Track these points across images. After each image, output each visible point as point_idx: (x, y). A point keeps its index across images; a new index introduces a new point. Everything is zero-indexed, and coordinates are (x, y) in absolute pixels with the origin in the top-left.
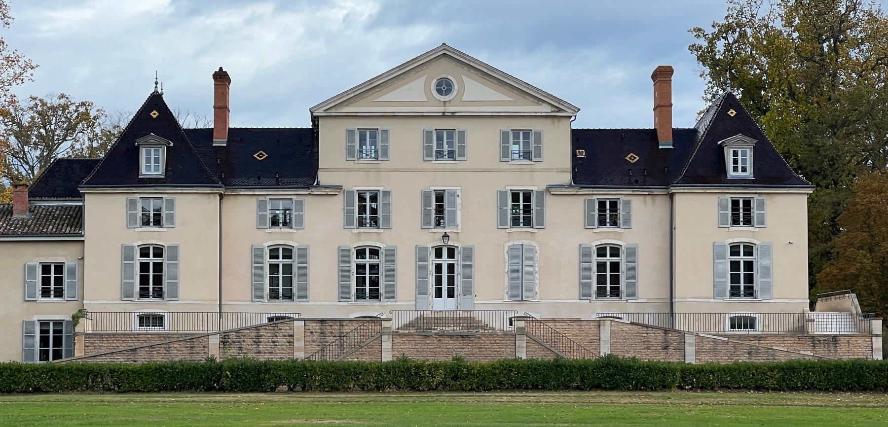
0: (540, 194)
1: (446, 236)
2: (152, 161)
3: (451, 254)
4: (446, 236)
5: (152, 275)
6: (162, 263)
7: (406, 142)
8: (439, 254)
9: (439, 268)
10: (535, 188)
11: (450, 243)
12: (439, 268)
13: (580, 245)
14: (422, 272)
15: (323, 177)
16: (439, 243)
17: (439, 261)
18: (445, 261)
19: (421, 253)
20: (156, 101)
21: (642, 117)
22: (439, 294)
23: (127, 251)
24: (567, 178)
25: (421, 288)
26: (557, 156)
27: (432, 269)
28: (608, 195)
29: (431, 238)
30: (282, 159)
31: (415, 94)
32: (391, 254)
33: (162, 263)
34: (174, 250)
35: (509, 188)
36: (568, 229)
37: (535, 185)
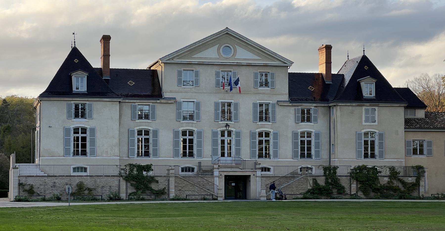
0: (273, 105)
1: (227, 125)
2: (80, 82)
3: (229, 134)
4: (227, 125)
5: (81, 144)
6: (86, 137)
7: (208, 77)
8: (223, 135)
9: (223, 142)
10: (271, 102)
11: (230, 129)
12: (223, 142)
13: (293, 132)
14: (214, 142)
15: (166, 95)
16: (225, 128)
17: (223, 138)
18: (226, 139)
19: (215, 134)
20: (75, 53)
21: (321, 69)
22: (223, 155)
23: (67, 131)
24: (286, 97)
25: (214, 152)
26: (282, 87)
27: (220, 142)
28: (306, 106)
29: (220, 126)
30: (145, 85)
32: (200, 134)
33: (86, 137)
34: (93, 130)
35: (258, 102)
36: (287, 123)
37: (272, 100)
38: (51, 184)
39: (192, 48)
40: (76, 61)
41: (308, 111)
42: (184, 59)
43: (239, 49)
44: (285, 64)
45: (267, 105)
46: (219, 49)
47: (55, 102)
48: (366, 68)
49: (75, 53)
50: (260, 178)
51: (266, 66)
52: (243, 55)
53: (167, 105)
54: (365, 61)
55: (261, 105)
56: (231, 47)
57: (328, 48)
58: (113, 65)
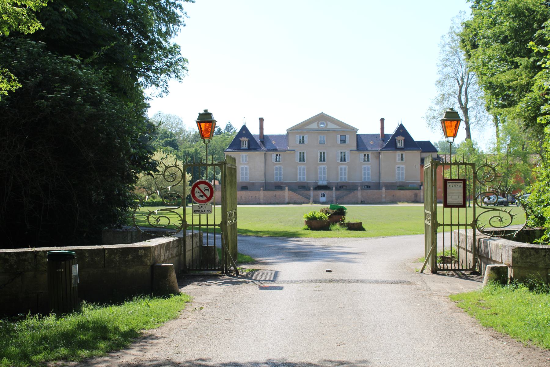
20: (244, 128)
24: (355, 148)
28: (366, 153)
31: (314, 126)
40: (244, 132)
41: (368, 155)
42: (300, 130)
43: (329, 123)
44: (354, 130)
45: (344, 152)
46: (318, 124)
48: (401, 131)
49: (244, 128)
51: (343, 131)
52: (331, 126)
54: (401, 127)
55: (341, 153)
57: (382, 120)
58: (265, 133)
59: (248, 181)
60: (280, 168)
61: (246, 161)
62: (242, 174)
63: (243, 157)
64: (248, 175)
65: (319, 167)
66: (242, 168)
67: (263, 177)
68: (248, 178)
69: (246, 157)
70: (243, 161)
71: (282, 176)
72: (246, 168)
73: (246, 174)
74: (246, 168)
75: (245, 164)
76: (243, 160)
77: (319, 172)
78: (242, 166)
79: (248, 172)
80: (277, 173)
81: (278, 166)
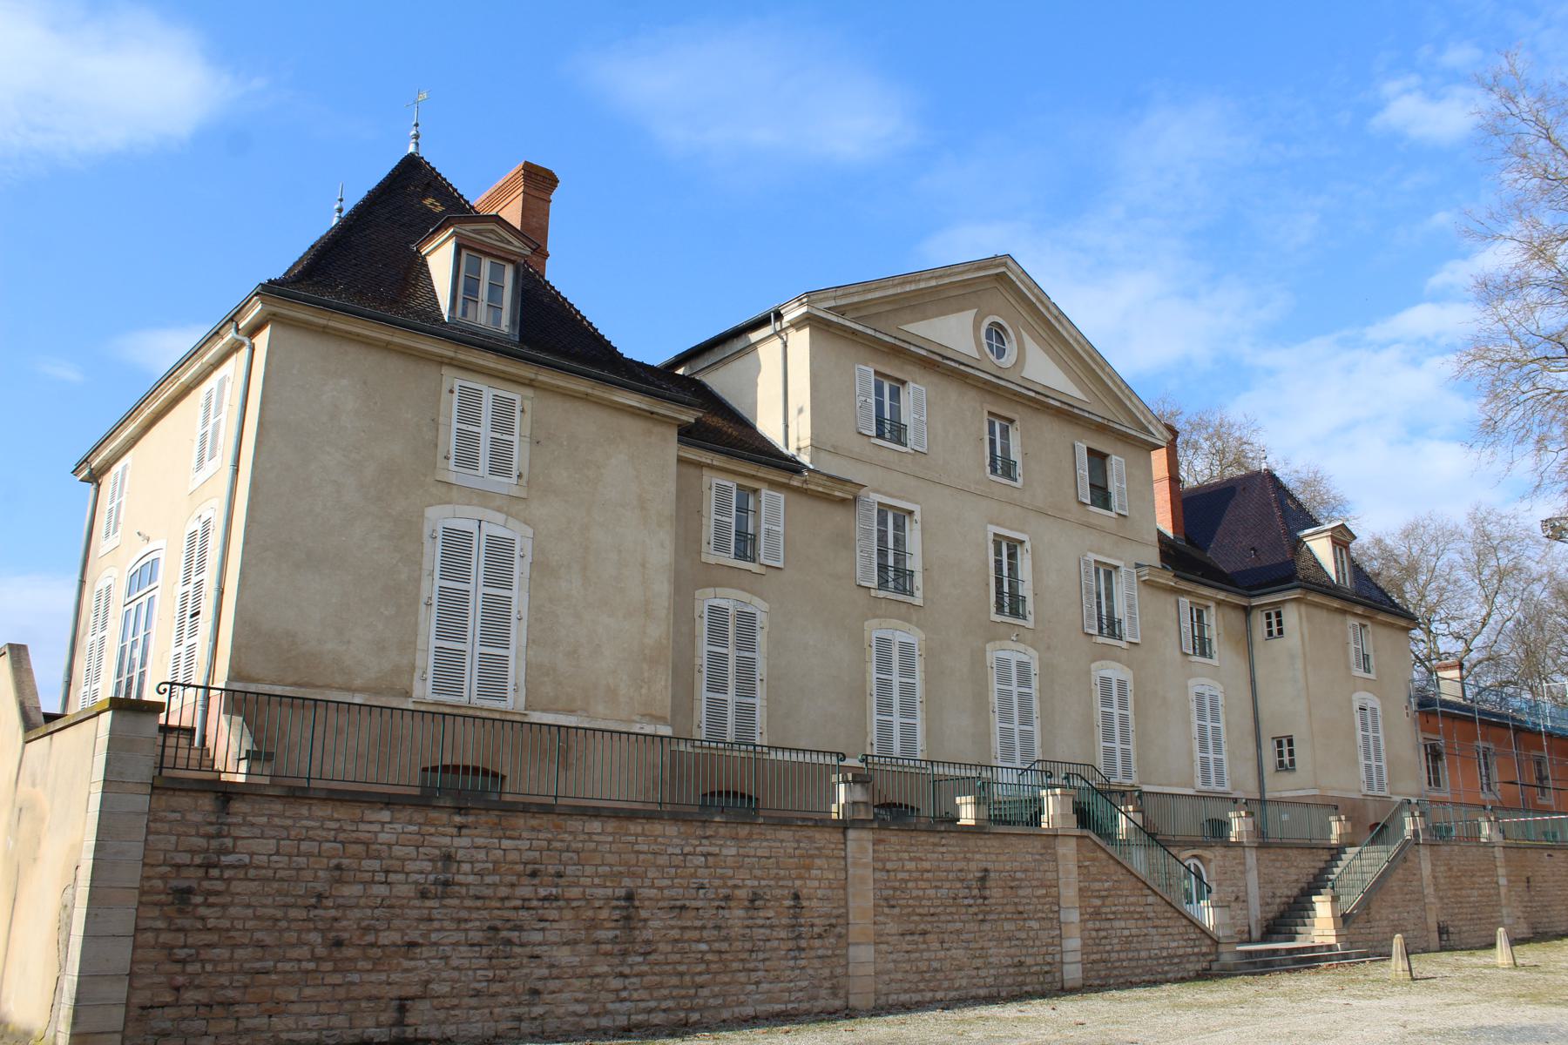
38: (421, 869)
39: (908, 288)
43: (1031, 345)
47: (353, 353)
50: (1254, 852)
52: (1042, 370)
53: (822, 507)
56: (1010, 331)
59: (513, 701)
60: (747, 621)
61: (500, 465)
62: (453, 605)
63: (469, 413)
64: (517, 634)
65: (993, 653)
66: (456, 543)
67: (661, 687)
68: (515, 672)
69: (503, 420)
70: (467, 459)
71: (759, 701)
72: (500, 551)
73: (497, 613)
74: (500, 551)
75: (483, 497)
76: (468, 442)
77: (994, 698)
78: (462, 518)
79: (518, 598)
80: (717, 661)
81: (729, 599)
